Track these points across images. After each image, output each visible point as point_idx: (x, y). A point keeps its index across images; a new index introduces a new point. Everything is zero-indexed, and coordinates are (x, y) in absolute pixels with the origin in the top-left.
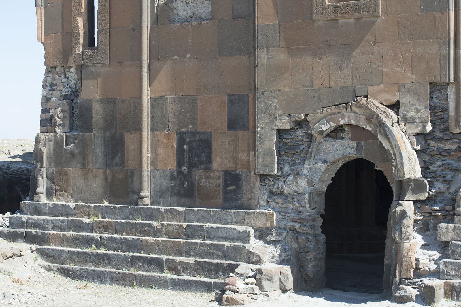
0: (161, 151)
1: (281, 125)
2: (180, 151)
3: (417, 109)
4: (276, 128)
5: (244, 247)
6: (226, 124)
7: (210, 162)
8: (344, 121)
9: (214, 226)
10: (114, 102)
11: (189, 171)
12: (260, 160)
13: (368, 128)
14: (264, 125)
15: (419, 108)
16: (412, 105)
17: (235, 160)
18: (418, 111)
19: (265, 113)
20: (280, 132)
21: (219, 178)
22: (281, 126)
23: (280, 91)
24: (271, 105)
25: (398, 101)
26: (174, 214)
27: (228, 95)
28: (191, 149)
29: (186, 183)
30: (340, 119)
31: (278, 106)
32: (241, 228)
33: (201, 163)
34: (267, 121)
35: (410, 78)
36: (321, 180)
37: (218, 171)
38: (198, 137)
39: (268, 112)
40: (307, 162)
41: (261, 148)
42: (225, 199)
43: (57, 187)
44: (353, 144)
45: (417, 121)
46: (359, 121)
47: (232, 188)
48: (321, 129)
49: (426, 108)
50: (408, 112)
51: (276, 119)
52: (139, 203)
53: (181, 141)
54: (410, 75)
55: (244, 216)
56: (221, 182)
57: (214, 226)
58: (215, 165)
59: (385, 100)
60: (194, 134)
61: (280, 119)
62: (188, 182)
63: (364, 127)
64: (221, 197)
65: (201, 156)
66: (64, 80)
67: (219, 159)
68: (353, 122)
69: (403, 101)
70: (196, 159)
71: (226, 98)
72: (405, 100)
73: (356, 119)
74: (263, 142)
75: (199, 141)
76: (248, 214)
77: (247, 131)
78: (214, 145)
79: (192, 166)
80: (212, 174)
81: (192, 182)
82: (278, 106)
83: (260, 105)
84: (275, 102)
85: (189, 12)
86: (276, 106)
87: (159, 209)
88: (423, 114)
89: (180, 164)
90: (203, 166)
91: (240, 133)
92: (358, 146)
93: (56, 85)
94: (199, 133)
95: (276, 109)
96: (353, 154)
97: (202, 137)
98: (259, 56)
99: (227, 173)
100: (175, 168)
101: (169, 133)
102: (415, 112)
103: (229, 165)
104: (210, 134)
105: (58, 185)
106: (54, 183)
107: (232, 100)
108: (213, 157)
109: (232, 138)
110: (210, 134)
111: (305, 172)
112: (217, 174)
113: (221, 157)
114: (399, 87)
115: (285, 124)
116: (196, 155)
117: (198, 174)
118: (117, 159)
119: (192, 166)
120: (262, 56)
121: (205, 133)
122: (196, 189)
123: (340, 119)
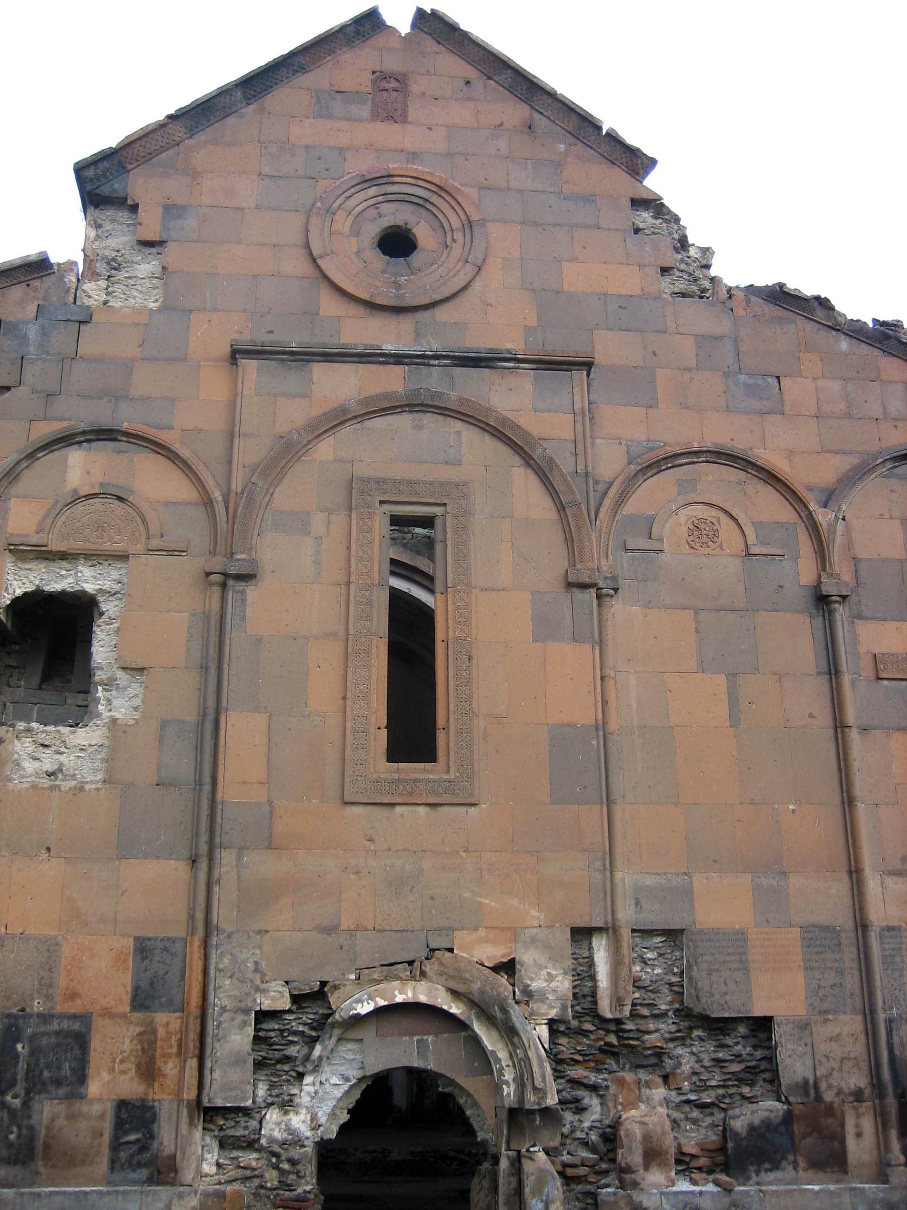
1: (267, 1002)
3: (549, 974)
6: (127, 998)
8: (404, 996)
11: (26, 1104)
12: (216, 1075)
15: (554, 973)
16: (541, 967)
18: (551, 978)
19: (231, 977)
20: (263, 1016)
21: (102, 1116)
22: (267, 1004)
25: (513, 960)
27: (136, 939)
28: (35, 1052)
29: (15, 1129)
30: (396, 992)
33: (58, 1083)
35: (535, 915)
36: (332, 1115)
37: (100, 1100)
38: (55, 1026)
40: (308, 1079)
42: (114, 1164)
45: (551, 997)
46: (436, 997)
47: (132, 1137)
48: (355, 1012)
49: (565, 973)
50: (532, 979)
54: (534, 913)
55: (171, 1202)
56: (108, 1126)
58: (94, 1088)
59: (489, 958)
60: (45, 1018)
62: (20, 1127)
63: (445, 1007)
65: (59, 1068)
67: (105, 1076)
70: (46, 1074)
71: (130, 943)
72: (527, 957)
73: (429, 994)
74: (225, 1037)
75: (57, 1033)
77: (177, 1014)
78: (96, 1044)
80: (85, 1108)
81: (31, 1128)
88: (562, 983)
90: (62, 1091)
94: (62, 1017)
97: (65, 1025)
98: (224, 862)
99: (122, 1105)
102: (546, 981)
108: (91, 1071)
109: (139, 1029)
110: (85, 1018)
112: (97, 1108)
113: (112, 1070)
116: (48, 1066)
121: (74, 1017)
122: (39, 1144)
123: (396, 992)
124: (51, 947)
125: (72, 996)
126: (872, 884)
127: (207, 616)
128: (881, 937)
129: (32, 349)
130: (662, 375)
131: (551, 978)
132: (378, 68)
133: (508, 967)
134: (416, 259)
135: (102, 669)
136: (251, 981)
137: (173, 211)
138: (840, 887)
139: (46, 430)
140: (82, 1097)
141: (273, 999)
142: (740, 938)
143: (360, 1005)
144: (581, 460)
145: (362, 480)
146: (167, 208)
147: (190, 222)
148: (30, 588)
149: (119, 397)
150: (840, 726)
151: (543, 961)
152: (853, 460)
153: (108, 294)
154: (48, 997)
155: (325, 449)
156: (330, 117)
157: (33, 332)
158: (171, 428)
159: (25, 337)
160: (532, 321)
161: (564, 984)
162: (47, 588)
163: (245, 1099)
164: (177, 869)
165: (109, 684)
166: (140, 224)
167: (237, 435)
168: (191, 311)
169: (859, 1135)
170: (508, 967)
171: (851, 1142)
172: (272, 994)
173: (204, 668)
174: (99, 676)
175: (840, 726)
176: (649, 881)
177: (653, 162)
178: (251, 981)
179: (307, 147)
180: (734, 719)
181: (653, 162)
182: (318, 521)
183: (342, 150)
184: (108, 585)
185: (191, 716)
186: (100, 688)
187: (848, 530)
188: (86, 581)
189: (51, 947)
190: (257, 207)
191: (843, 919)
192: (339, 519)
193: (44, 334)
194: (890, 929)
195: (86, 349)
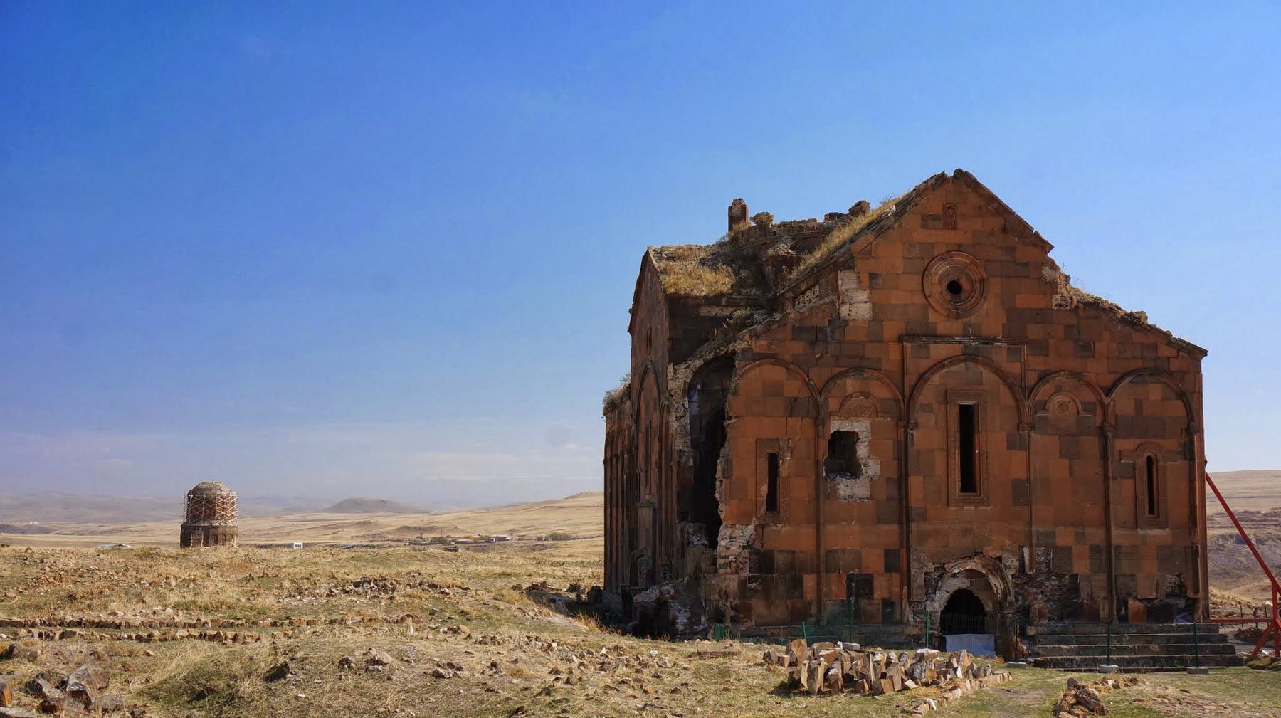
2: (849, 587)
7: (872, 594)
10: (793, 552)
12: (914, 591)
13: (983, 572)
16: (1010, 558)
17: (891, 593)
21: (879, 604)
24: (921, 557)
28: (856, 585)
39: (918, 560)
40: (937, 592)
41: (914, 585)
44: (965, 580)
53: (850, 578)
60: (860, 575)
64: (880, 619)
66: (741, 534)
67: (879, 593)
68: (974, 568)
69: (1005, 555)
79: (858, 597)
85: (848, 492)
89: (849, 597)
91: (894, 575)
92: (971, 582)
93: (735, 538)
96: (964, 586)
99: (884, 600)
103: (886, 596)
107: (887, 553)
111: (937, 598)
112: (877, 602)
114: (1002, 548)
117: (863, 602)
118: (797, 593)
119: (858, 597)
124: (858, 553)
126: (1114, 532)
127: (899, 442)
128: (1115, 549)
130: (1051, 341)
131: (1012, 561)
133: (999, 559)
134: (963, 295)
137: (873, 276)
138: (1102, 532)
139: (837, 370)
140: (873, 599)
142: (1070, 549)
144: (1023, 381)
147: (880, 281)
148: (835, 430)
149: (862, 357)
150: (1106, 478)
151: (1010, 556)
152: (1118, 376)
154: (858, 568)
155: (936, 379)
156: (927, 228)
157: (828, 330)
159: (825, 334)
160: (1005, 321)
161: (1017, 564)
162: (842, 430)
164: (895, 527)
169: (1104, 609)
170: (999, 559)
171: (1101, 612)
173: (899, 459)
175: (1106, 478)
176: (1041, 529)
177: (1052, 247)
180: (1071, 475)
181: (1052, 247)
182: (935, 406)
183: (932, 244)
185: (896, 477)
187: (1115, 405)
189: (858, 553)
190: (903, 273)
191: (1103, 544)
192: (943, 407)
193: (833, 332)
194: (1117, 546)
195: (848, 338)
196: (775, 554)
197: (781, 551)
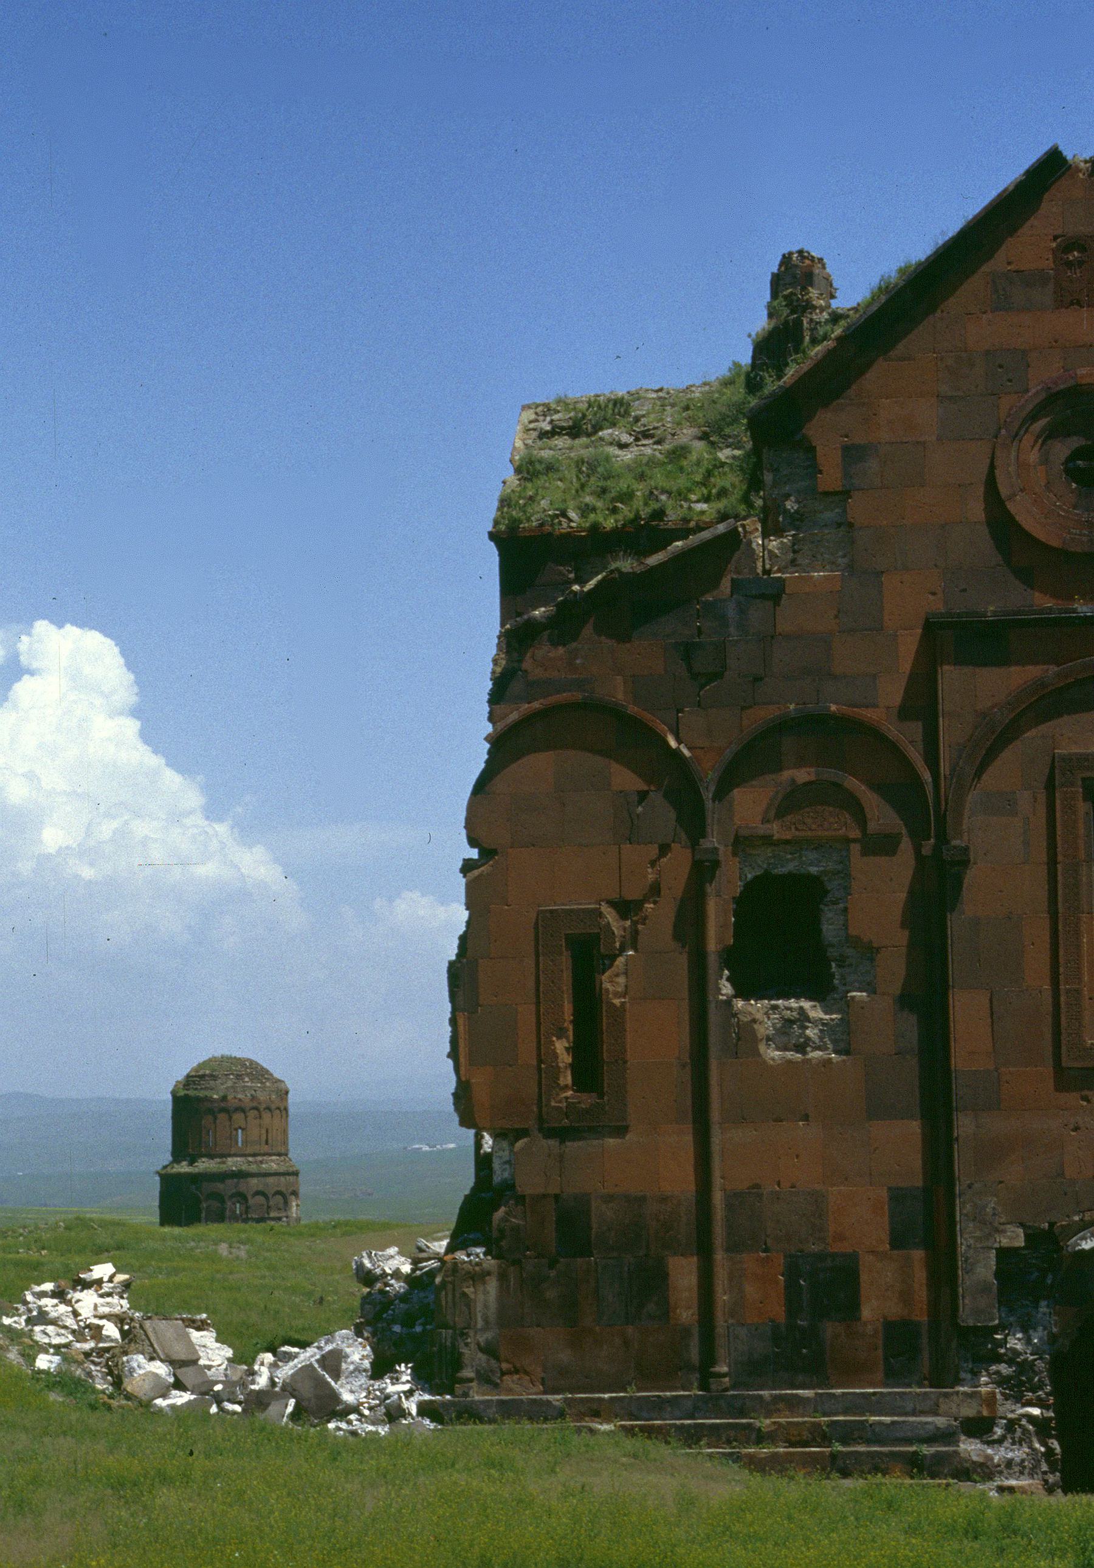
0: (751, 1290)
1: (1005, 1241)
4: (997, 1245)
5: (956, 1453)
9: (887, 1419)
14: (972, 1241)
19: (973, 1220)
20: (1004, 1254)
22: (1005, 1242)
23: (1001, 1182)
26: (794, 1404)
27: (889, 1189)
31: (1000, 1209)
32: (941, 1421)
34: (978, 1234)
41: (966, 1282)
43: (505, 1366)
51: (997, 1231)
52: (713, 1387)
55: (938, 1400)
57: (887, 1419)
58: (866, 1313)
61: (1004, 1231)
71: (884, 1193)
76: (946, 1395)
82: (1000, 1209)
83: (963, 1208)
84: (992, 1203)
86: (994, 1208)
87: (761, 1396)
94: (834, 1256)
95: (994, 1214)
98: (960, 1123)
100: (782, 1319)
101: (767, 1257)
104: (853, 1258)
105: (507, 1361)
106: (498, 1359)
110: (853, 1258)
112: (869, 1329)
115: (1014, 1237)
118: (651, 1307)
120: (964, 1125)
125: (840, 1237)
129: (732, 630)
132: (1059, 232)
135: (833, 946)
136: (990, 1223)
137: (853, 454)
141: (1011, 1238)
143: (1084, 1242)
145: (1063, 758)
146: (846, 449)
153: (794, 552)
157: (731, 612)
158: (875, 706)
163: (993, 1319)
165: (842, 962)
166: (821, 472)
167: (940, 714)
168: (882, 572)
172: (1009, 1234)
174: (832, 953)
178: (990, 1223)
179: (987, 353)
184: (831, 866)
186: (833, 965)
188: (810, 865)
196: (594, 1204)
197: (609, 1198)
